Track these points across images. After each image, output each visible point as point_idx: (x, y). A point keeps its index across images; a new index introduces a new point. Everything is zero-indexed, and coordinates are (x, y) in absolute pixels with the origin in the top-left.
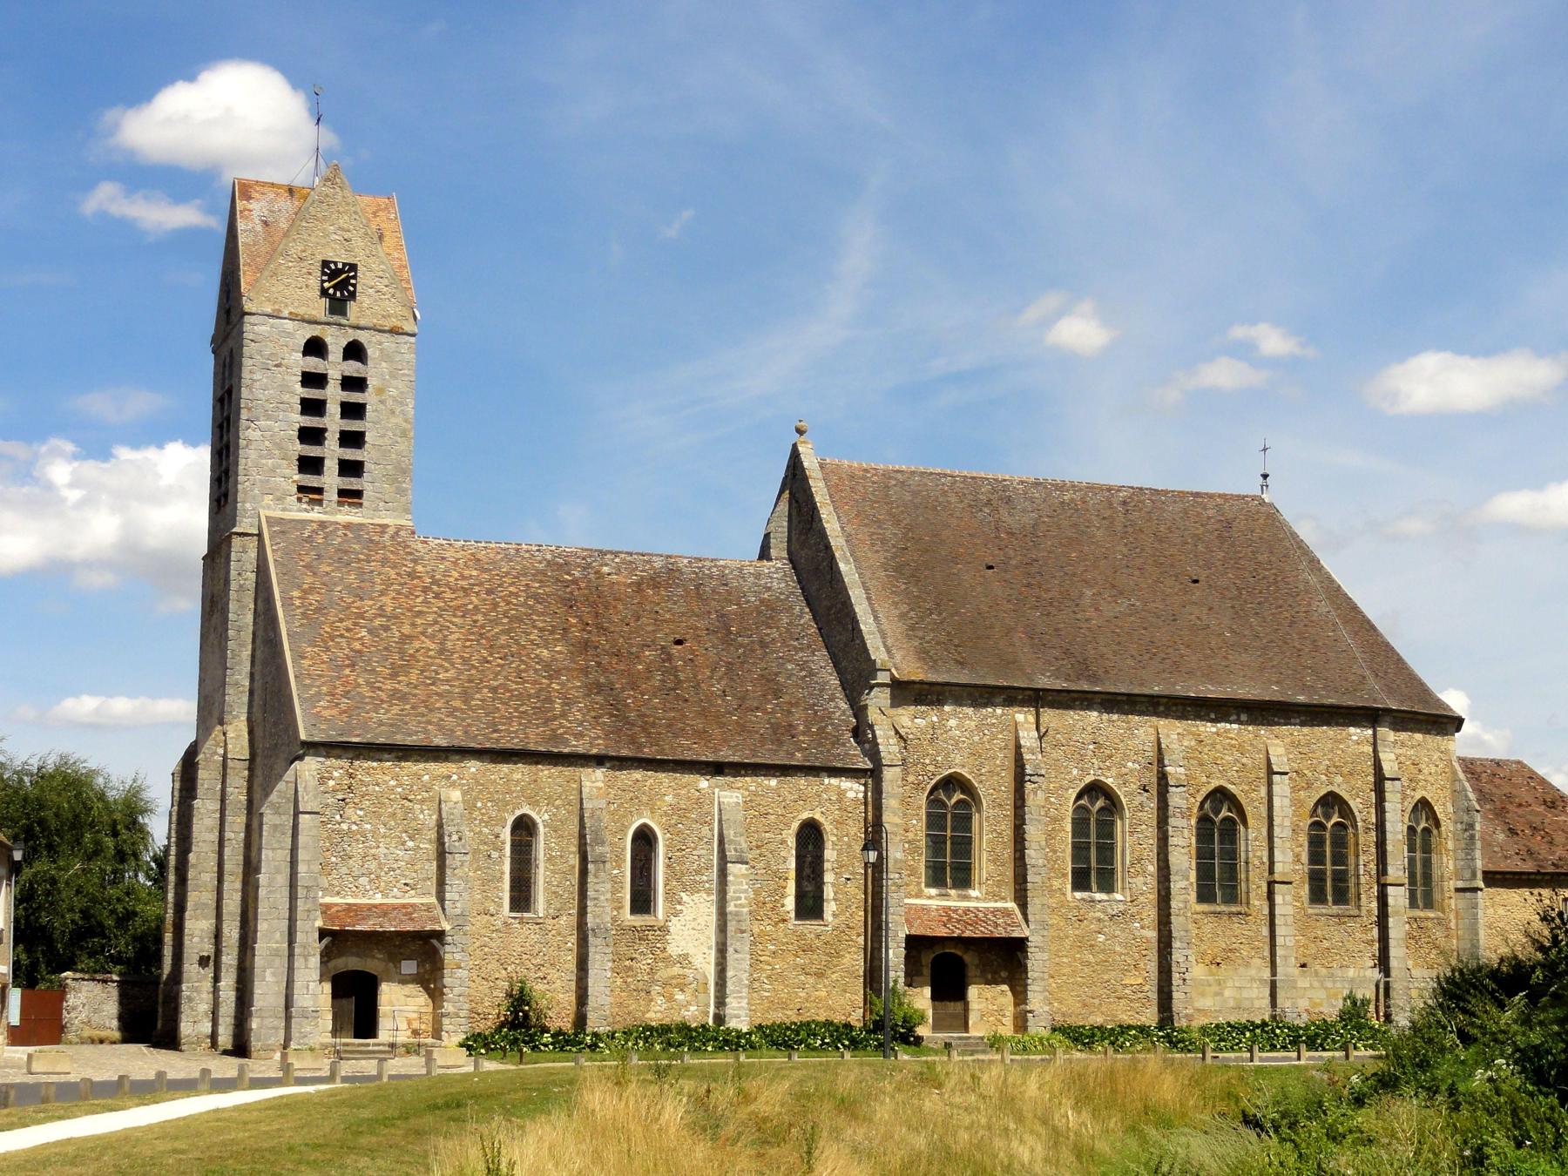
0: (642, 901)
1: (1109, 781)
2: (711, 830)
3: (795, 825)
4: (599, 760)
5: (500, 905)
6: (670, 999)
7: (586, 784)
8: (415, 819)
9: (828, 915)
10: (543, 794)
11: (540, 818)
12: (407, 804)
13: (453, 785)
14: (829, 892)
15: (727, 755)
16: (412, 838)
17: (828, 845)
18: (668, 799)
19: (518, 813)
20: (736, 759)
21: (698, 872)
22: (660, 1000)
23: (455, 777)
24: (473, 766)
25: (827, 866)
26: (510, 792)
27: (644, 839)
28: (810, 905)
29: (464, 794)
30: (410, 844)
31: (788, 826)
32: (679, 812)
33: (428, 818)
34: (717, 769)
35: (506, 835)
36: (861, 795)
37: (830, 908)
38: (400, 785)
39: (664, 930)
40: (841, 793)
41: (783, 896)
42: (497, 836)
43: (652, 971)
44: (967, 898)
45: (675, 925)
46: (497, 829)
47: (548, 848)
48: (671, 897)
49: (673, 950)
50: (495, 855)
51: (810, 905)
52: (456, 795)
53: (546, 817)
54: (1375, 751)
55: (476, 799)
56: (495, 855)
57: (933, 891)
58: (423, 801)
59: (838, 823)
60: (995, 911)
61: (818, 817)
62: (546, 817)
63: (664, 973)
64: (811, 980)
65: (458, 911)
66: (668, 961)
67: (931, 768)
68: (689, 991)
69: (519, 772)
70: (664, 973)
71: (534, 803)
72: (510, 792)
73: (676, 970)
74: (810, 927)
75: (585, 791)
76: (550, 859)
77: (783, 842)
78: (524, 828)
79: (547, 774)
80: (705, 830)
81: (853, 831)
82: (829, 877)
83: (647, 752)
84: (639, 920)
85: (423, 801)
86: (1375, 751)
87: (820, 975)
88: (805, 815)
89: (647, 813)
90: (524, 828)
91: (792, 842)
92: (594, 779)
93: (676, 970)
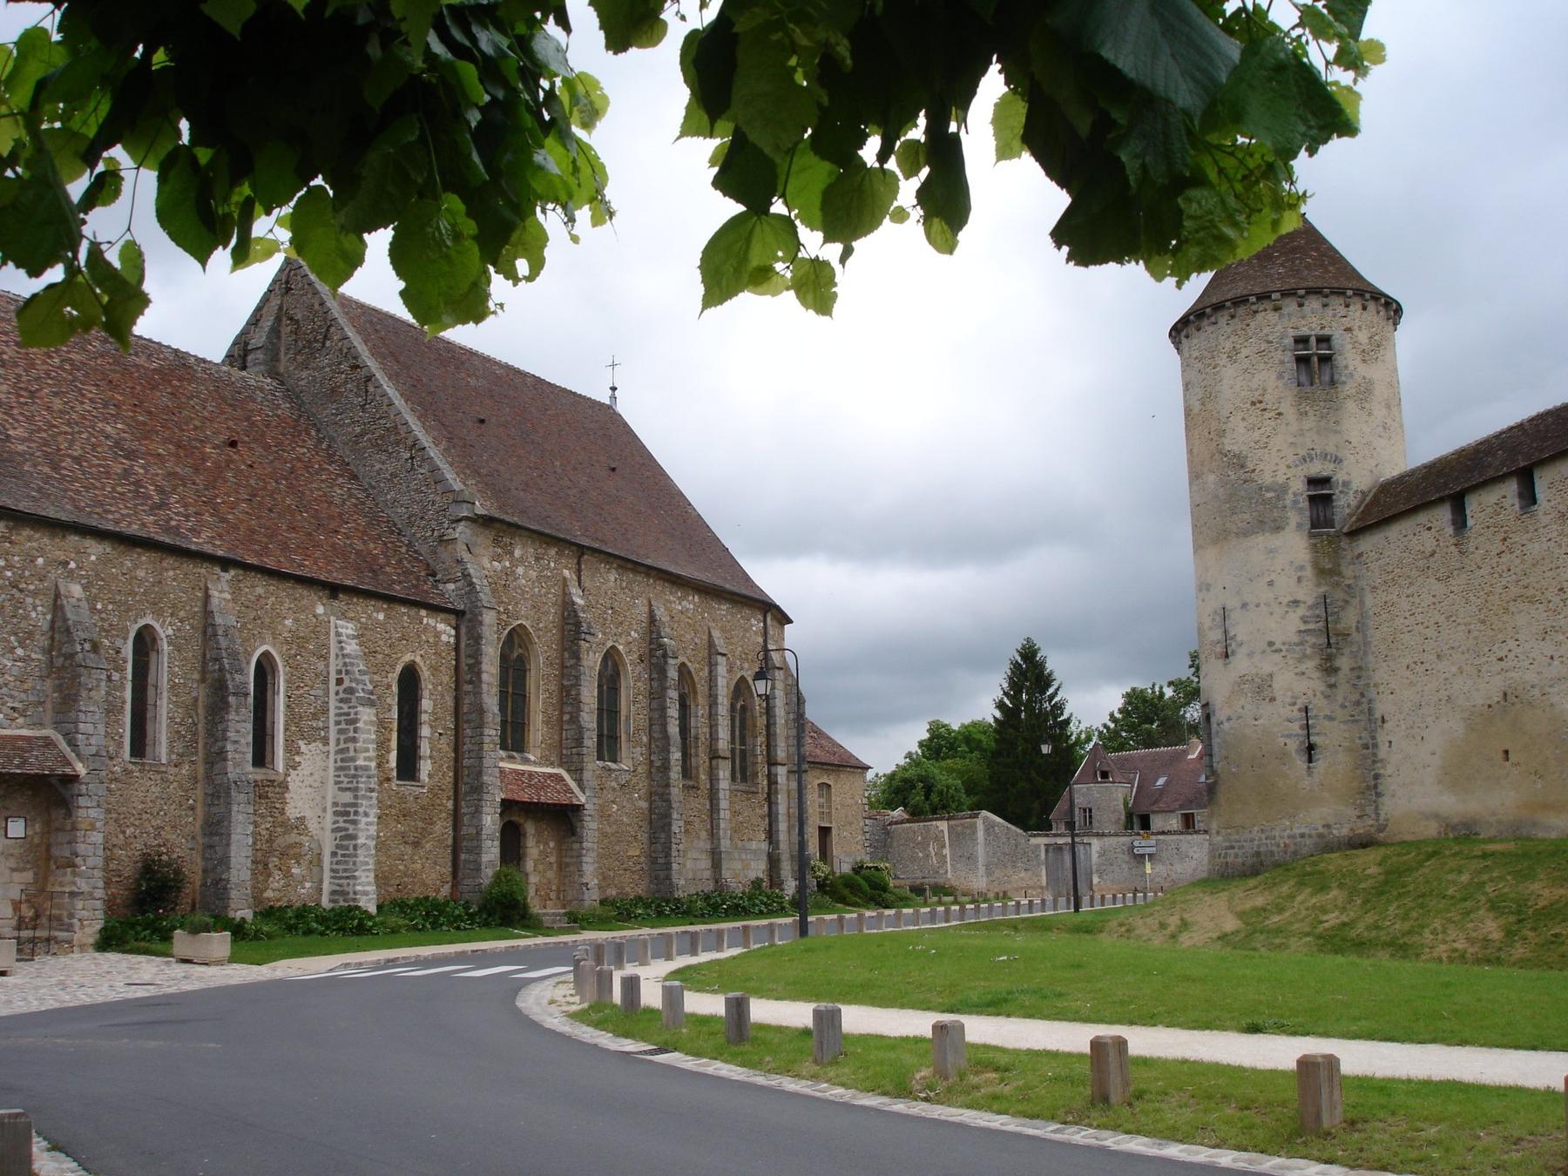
0: (261, 756)
1: (621, 648)
2: (327, 666)
3: (399, 669)
4: (226, 564)
5: (120, 745)
6: (288, 874)
7: (214, 593)
8: (26, 617)
9: (424, 775)
10: (163, 603)
11: (164, 631)
12: (17, 595)
13: (79, 575)
14: (425, 748)
15: (336, 577)
16: (22, 644)
17: (426, 693)
18: (288, 622)
19: (142, 623)
20: (349, 583)
21: (315, 716)
22: (277, 875)
23: (72, 565)
24: (95, 550)
25: (424, 717)
26: (132, 593)
27: (265, 670)
28: (408, 767)
29: (85, 588)
30: (20, 652)
31: (393, 667)
32: (297, 642)
33: (39, 616)
34: (334, 590)
35: (128, 650)
36: (452, 640)
37: (425, 768)
38: (9, 567)
39: (284, 786)
40: (437, 635)
41: (388, 752)
42: (118, 652)
43: (270, 841)
44: (526, 761)
45: (294, 780)
46: (119, 643)
47: (172, 674)
48: (292, 749)
49: (292, 812)
50: (116, 676)
51: (408, 767)
52: (76, 590)
53: (170, 632)
54: (765, 641)
55: (95, 599)
56: (116, 676)
57: (503, 753)
58: (35, 594)
59: (434, 669)
60: (551, 775)
61: (418, 659)
62: (170, 632)
63: (281, 842)
64: (409, 850)
65: (93, 750)
66: (288, 827)
67: (504, 617)
68: (304, 863)
69: (142, 566)
70: (281, 842)
71: (158, 613)
72: (132, 593)
73: (293, 838)
74: (408, 788)
75: (215, 602)
76: (173, 687)
77: (389, 686)
78: (145, 642)
79: (174, 573)
80: (321, 666)
81: (446, 679)
82: (425, 731)
83: (270, 563)
84: (259, 775)
85: (35, 594)
86: (765, 641)
87: (416, 844)
88: (408, 658)
89: (269, 638)
90: (145, 642)
91: (395, 689)
92: (221, 588)
93: (293, 838)
